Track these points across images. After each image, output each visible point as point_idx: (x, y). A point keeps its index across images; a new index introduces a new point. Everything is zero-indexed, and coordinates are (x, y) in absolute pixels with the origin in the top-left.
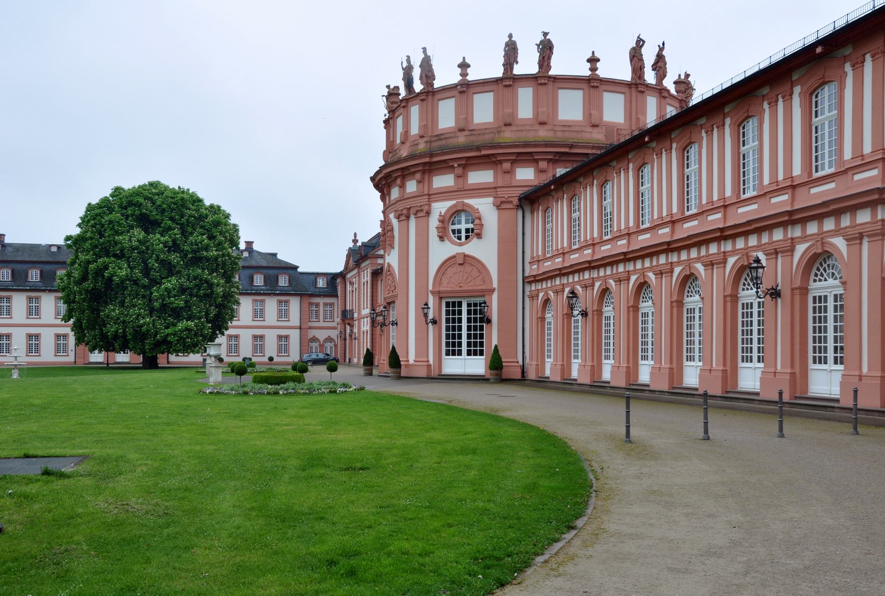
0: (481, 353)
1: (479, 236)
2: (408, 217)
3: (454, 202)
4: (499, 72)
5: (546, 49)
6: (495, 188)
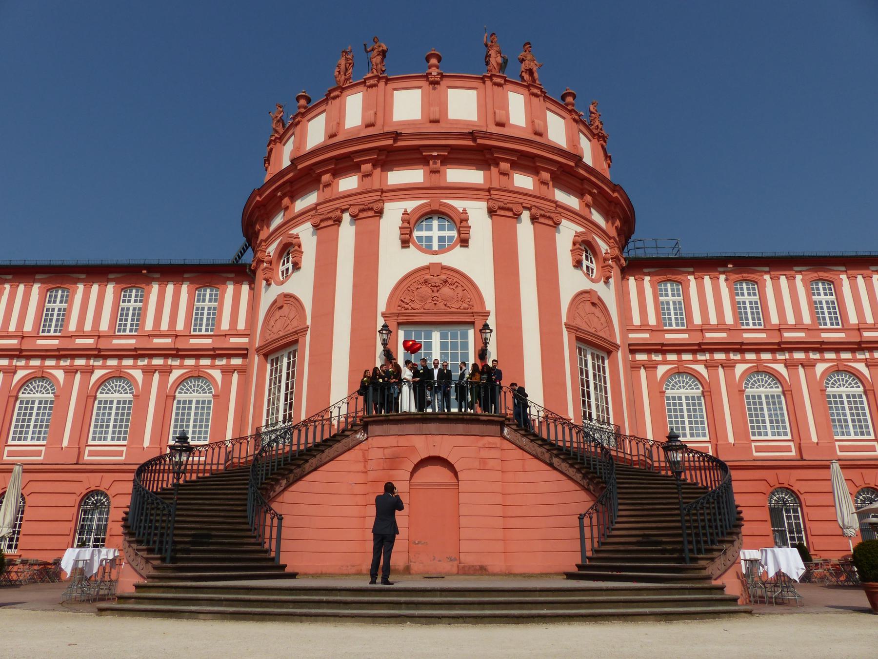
1: (464, 242)
2: (338, 221)
6: (489, 190)
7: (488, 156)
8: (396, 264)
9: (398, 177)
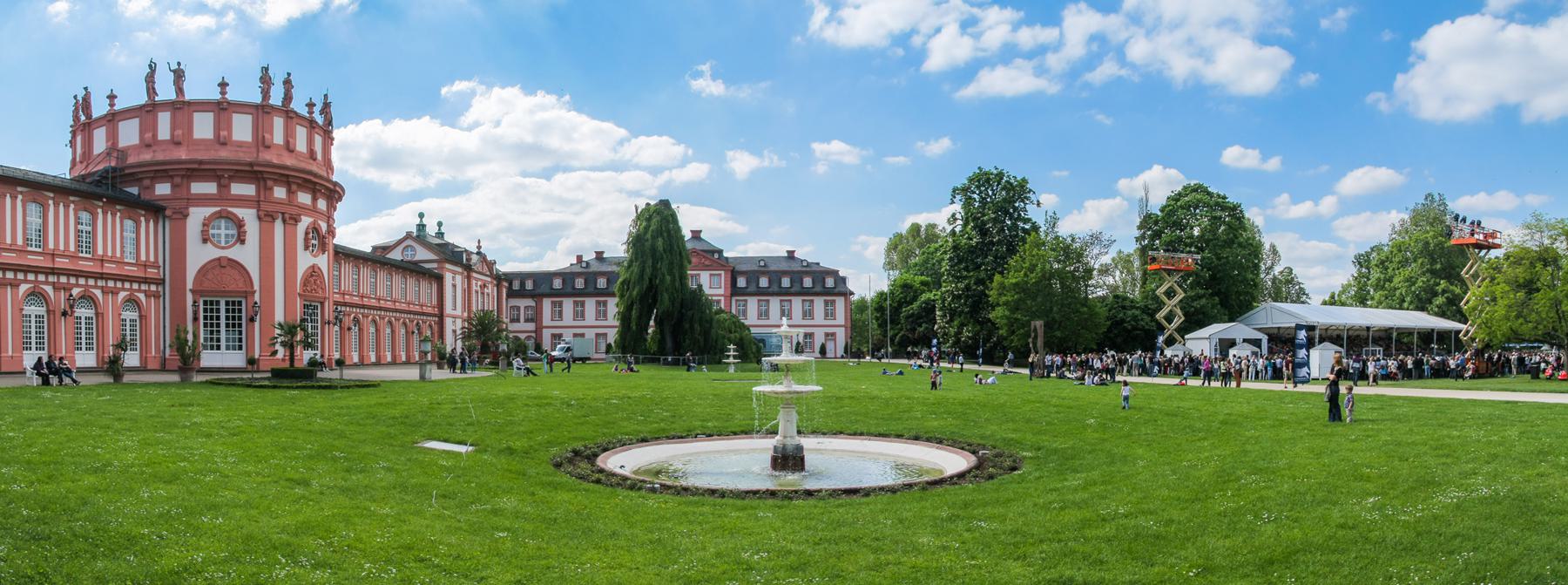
0: (240, 348)
8: (198, 255)
9: (198, 188)
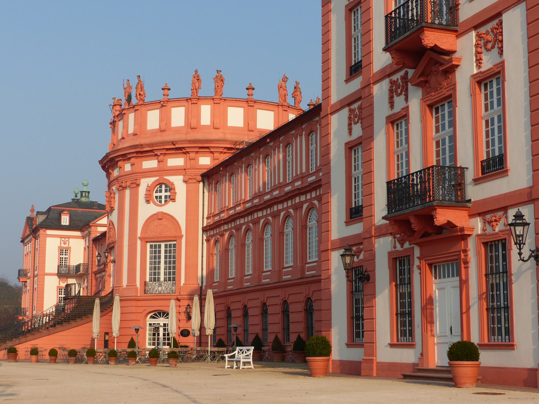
1: (173, 200)
2: (125, 188)
3: (158, 178)
4: (189, 95)
5: (220, 80)
6: (185, 170)
7: (184, 151)
8: (146, 211)
